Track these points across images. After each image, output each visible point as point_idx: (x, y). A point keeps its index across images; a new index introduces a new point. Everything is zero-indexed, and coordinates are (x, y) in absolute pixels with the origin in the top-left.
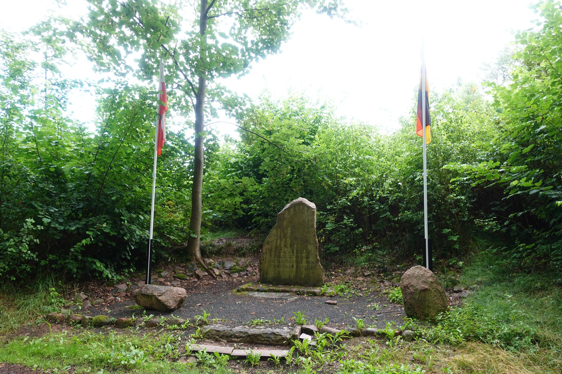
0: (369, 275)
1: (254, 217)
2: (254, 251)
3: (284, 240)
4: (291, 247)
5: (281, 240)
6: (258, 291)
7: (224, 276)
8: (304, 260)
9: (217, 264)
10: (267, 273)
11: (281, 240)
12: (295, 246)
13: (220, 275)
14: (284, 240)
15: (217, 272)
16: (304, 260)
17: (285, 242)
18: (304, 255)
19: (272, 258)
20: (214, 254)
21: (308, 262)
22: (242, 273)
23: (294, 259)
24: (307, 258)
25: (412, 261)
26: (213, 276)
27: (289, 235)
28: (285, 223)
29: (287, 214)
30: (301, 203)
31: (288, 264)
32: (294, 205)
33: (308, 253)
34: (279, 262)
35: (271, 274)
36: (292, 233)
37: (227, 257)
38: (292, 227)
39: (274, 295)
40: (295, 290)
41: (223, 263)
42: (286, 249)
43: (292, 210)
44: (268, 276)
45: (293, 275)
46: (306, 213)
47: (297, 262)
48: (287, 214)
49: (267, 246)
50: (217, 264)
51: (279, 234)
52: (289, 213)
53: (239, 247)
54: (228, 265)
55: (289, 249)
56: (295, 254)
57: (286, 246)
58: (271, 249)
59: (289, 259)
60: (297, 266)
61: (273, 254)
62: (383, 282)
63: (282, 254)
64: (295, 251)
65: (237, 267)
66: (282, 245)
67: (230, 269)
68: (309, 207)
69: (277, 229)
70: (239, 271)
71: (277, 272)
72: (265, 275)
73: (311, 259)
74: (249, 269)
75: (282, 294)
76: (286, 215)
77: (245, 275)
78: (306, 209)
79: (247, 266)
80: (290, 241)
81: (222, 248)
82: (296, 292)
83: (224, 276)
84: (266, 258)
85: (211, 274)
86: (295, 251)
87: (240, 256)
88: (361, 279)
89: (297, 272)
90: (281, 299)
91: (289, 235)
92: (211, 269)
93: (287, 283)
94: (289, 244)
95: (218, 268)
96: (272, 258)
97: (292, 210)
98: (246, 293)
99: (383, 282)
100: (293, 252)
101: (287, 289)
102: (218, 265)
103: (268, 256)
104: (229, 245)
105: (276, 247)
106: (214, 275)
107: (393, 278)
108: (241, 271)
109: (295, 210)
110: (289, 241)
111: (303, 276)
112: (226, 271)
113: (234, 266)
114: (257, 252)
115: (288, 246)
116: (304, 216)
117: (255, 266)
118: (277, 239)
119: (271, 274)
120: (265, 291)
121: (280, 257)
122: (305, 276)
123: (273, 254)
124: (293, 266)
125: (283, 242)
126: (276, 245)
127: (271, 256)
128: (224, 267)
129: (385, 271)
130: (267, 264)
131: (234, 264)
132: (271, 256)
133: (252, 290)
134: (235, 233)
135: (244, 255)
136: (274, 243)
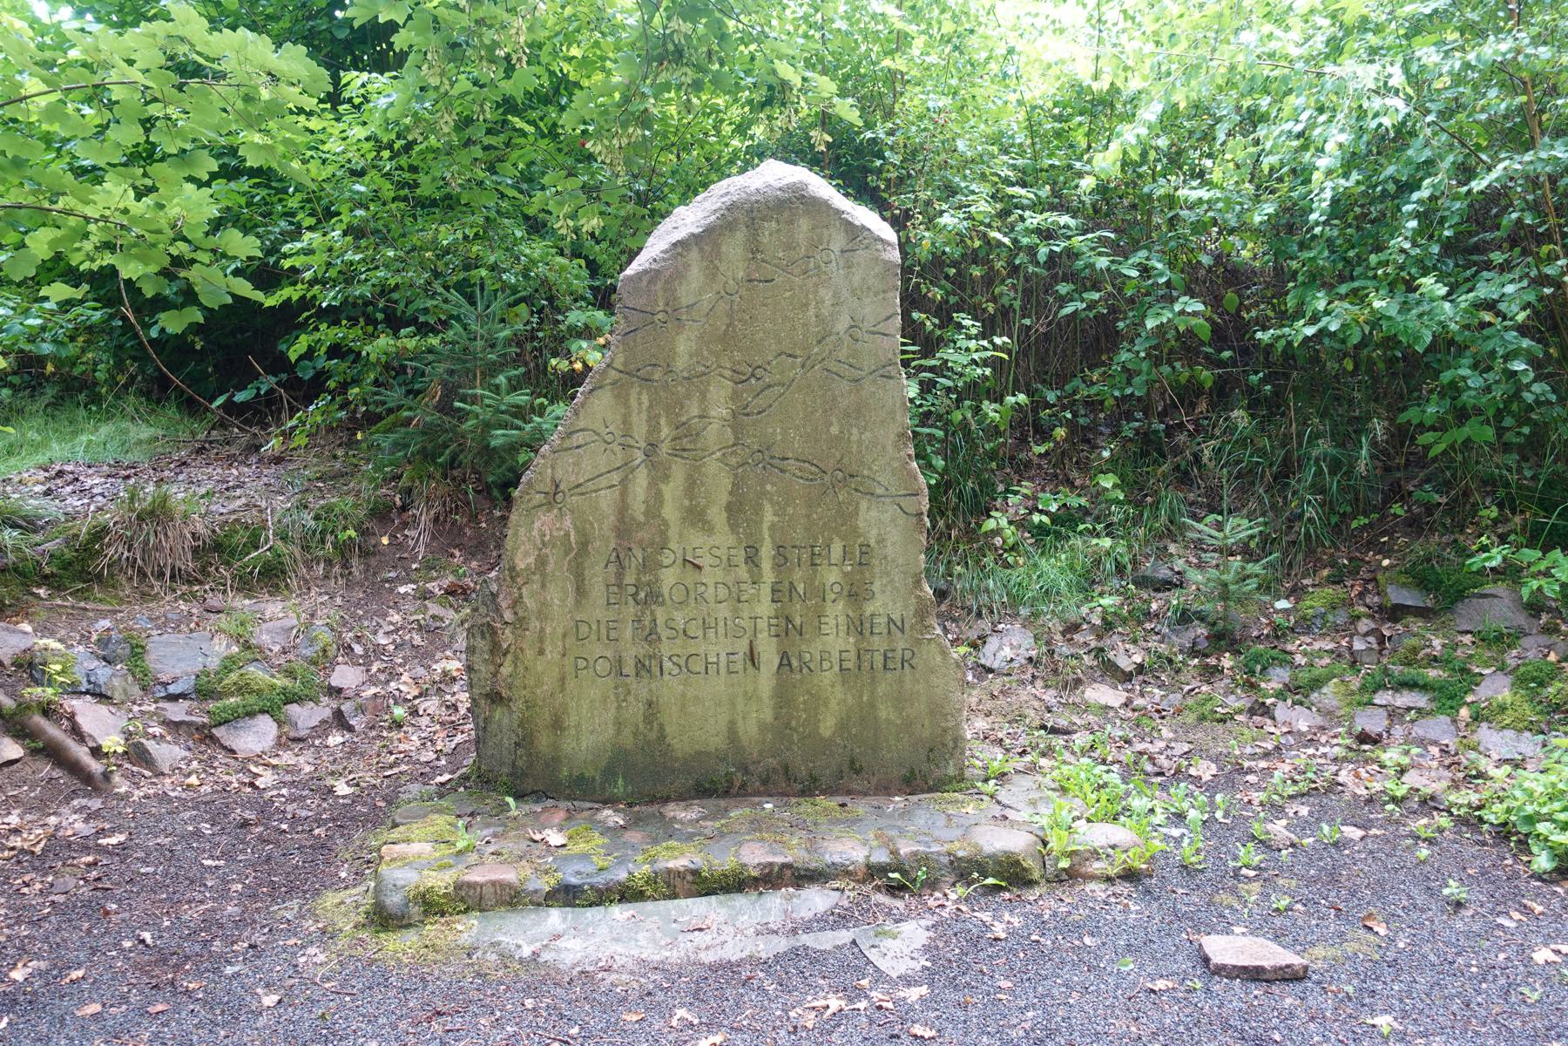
0: (1140, 668)
1: (303, 327)
2: (344, 549)
3: (678, 471)
4: (733, 527)
5: (660, 473)
6: (567, 895)
7: (167, 753)
8: (836, 612)
9: (84, 662)
10: (557, 725)
11: (660, 473)
12: (769, 516)
13: (137, 755)
14: (678, 471)
15: (103, 726)
16: (836, 612)
17: (691, 485)
18: (832, 576)
19: (597, 609)
20: (46, 580)
21: (859, 627)
22: (306, 716)
23: (765, 608)
24: (856, 594)
25: (1354, 573)
26: (74, 768)
27: (715, 433)
28: (684, 346)
29: (695, 274)
30: (795, 202)
31: (716, 648)
32: (749, 217)
33: (863, 557)
34: (652, 636)
35: (590, 727)
36: (739, 417)
37: (145, 596)
38: (739, 380)
39: (731, 930)
40: (850, 850)
41: (137, 652)
42: (696, 539)
43: (734, 248)
44: (568, 745)
45: (755, 719)
46: (836, 272)
47: (786, 628)
48: (695, 274)
49: (544, 521)
50: (84, 662)
51: (640, 430)
52: (712, 273)
53: (232, 527)
54: (183, 654)
55: (716, 543)
56: (768, 576)
57: (695, 516)
58: (584, 545)
59: (724, 611)
60: (784, 656)
61: (598, 576)
62: (1267, 711)
63: (669, 577)
64: (766, 552)
65: (257, 674)
66: (670, 512)
67: (203, 692)
68: (855, 232)
69: (621, 395)
70: (274, 705)
71: (635, 711)
72: (544, 741)
73: (885, 604)
74: (345, 676)
75: (774, 905)
76: (693, 286)
77: (323, 729)
78: (838, 242)
79: (324, 661)
80: (726, 482)
81: (99, 534)
82: (873, 872)
83: (167, 753)
84: (542, 616)
85: (53, 753)
86: (766, 552)
87: (245, 585)
88: (1104, 694)
89: (783, 696)
90: (796, 967)
91: (715, 433)
92: (47, 710)
93: (719, 783)
94: (724, 498)
95: (102, 697)
96: (597, 609)
97: (734, 248)
98: (468, 928)
99: (1267, 711)
100: (752, 559)
101: (793, 853)
102: (103, 673)
103: (558, 596)
104: (158, 514)
105: (624, 527)
106: (81, 753)
107: (1317, 684)
108: (292, 698)
109: (754, 250)
110: (718, 481)
111: (827, 726)
112: (177, 712)
113: (229, 664)
114: (365, 554)
115: (717, 515)
116: (826, 295)
117: (379, 651)
118: (627, 468)
119: (590, 727)
120: (628, 894)
121: (654, 597)
122: (842, 726)
123: (598, 576)
124: (752, 658)
125: (672, 491)
126: (623, 508)
127: (581, 591)
128: (148, 684)
129: (1223, 638)
130: (552, 653)
131: (222, 648)
132: (581, 591)
133: (512, 899)
134: (145, 432)
135: (272, 577)
136: (607, 500)
